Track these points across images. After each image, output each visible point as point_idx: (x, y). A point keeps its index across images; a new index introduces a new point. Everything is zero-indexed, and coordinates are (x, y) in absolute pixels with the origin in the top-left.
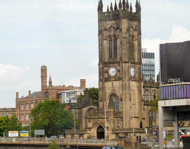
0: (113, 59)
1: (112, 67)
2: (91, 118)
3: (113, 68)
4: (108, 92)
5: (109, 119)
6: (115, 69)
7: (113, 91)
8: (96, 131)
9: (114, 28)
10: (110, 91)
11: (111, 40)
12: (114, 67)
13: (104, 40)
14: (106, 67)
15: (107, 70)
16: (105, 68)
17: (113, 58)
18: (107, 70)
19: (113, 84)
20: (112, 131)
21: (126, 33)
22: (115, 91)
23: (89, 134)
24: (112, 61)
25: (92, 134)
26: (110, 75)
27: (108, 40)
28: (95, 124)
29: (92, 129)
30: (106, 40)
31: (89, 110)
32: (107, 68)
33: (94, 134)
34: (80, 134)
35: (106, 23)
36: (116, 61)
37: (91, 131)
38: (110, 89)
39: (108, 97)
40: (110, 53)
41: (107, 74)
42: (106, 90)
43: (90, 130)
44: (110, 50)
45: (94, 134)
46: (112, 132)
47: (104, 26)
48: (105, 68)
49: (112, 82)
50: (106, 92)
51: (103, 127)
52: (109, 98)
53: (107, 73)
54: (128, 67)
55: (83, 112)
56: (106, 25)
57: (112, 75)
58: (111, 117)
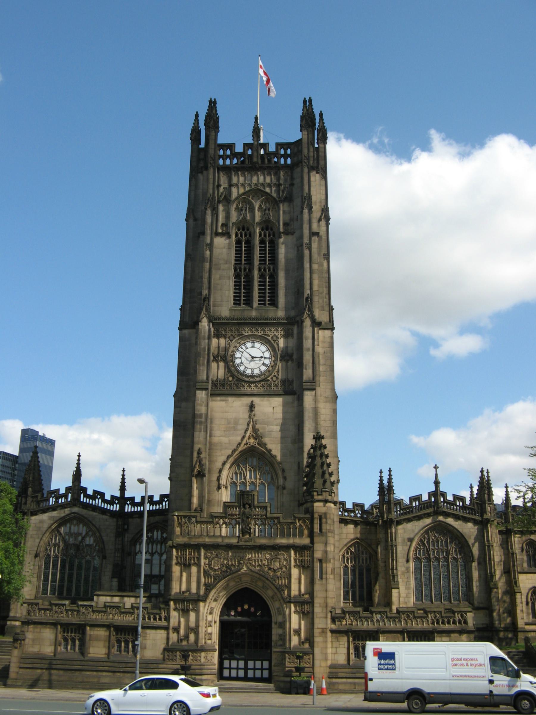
0: (256, 309)
1: (253, 338)
2: (197, 547)
3: (257, 345)
4: (225, 440)
5: (318, 555)
6: (264, 348)
7: (252, 440)
8: (216, 617)
9: (268, 197)
10: (239, 439)
11: (248, 242)
12: (264, 340)
13: (217, 234)
14: (218, 336)
15: (226, 349)
16: (214, 341)
17: (256, 304)
18: (226, 349)
19: (252, 407)
20: (329, 621)
21: (320, 220)
22: (266, 440)
23: (176, 630)
24: (254, 314)
25: (202, 630)
26: (242, 368)
27: (233, 237)
28: (217, 579)
29: (201, 604)
30: (227, 234)
31: (60, 526)
32: (222, 341)
33: (209, 630)
34: (120, 629)
35: (230, 179)
36: (271, 314)
37: (192, 615)
38: (235, 429)
39: (224, 464)
40: (237, 285)
41: (222, 364)
42: (217, 432)
43: (185, 612)
45: (209, 630)
46: (333, 627)
47: (219, 186)
48: (214, 341)
49: (247, 400)
50: (215, 440)
51: (267, 595)
52: (228, 466)
53: (224, 359)
54: (327, 345)
55: (31, 531)
56: (231, 185)
57: (249, 372)
58: (326, 544)
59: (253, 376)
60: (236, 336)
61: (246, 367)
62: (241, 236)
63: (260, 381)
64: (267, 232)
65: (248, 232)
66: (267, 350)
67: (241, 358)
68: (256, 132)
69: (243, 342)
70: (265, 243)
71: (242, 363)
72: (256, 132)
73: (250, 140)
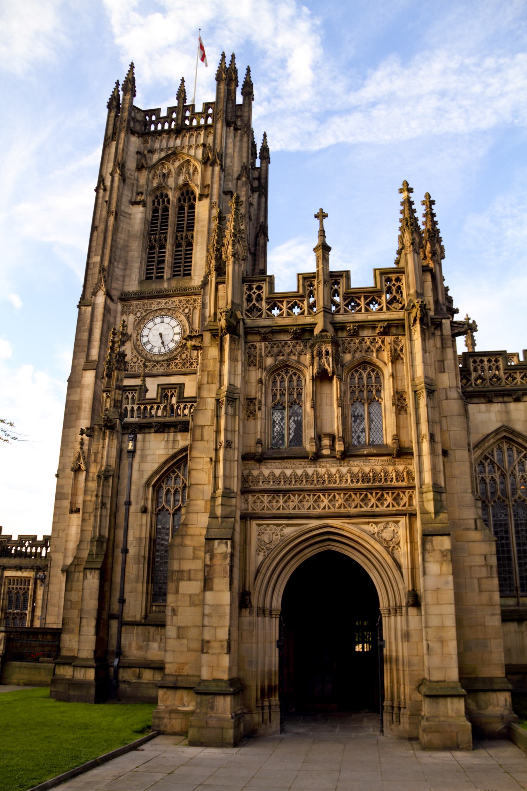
3: (167, 319)
44: (152, 247)
59: (159, 355)
60: (143, 312)
61: (153, 346)
62: (159, 204)
63: (167, 360)
64: (187, 197)
65: (166, 199)
66: (178, 325)
67: (148, 336)
68: (181, 95)
69: (151, 317)
70: (184, 209)
71: (149, 341)
72: (181, 95)
73: (174, 103)
